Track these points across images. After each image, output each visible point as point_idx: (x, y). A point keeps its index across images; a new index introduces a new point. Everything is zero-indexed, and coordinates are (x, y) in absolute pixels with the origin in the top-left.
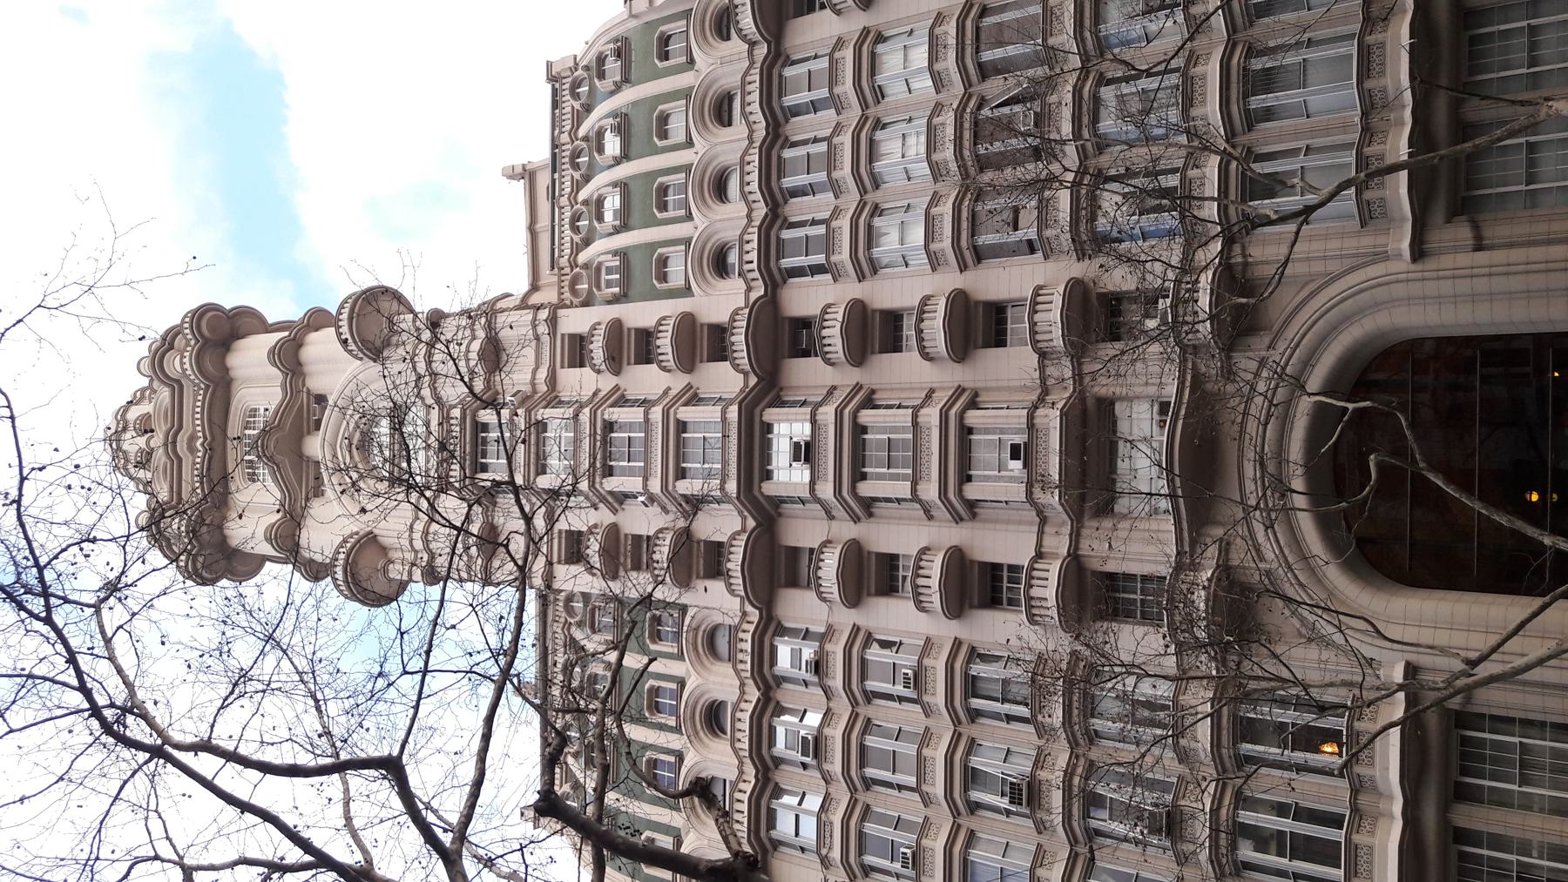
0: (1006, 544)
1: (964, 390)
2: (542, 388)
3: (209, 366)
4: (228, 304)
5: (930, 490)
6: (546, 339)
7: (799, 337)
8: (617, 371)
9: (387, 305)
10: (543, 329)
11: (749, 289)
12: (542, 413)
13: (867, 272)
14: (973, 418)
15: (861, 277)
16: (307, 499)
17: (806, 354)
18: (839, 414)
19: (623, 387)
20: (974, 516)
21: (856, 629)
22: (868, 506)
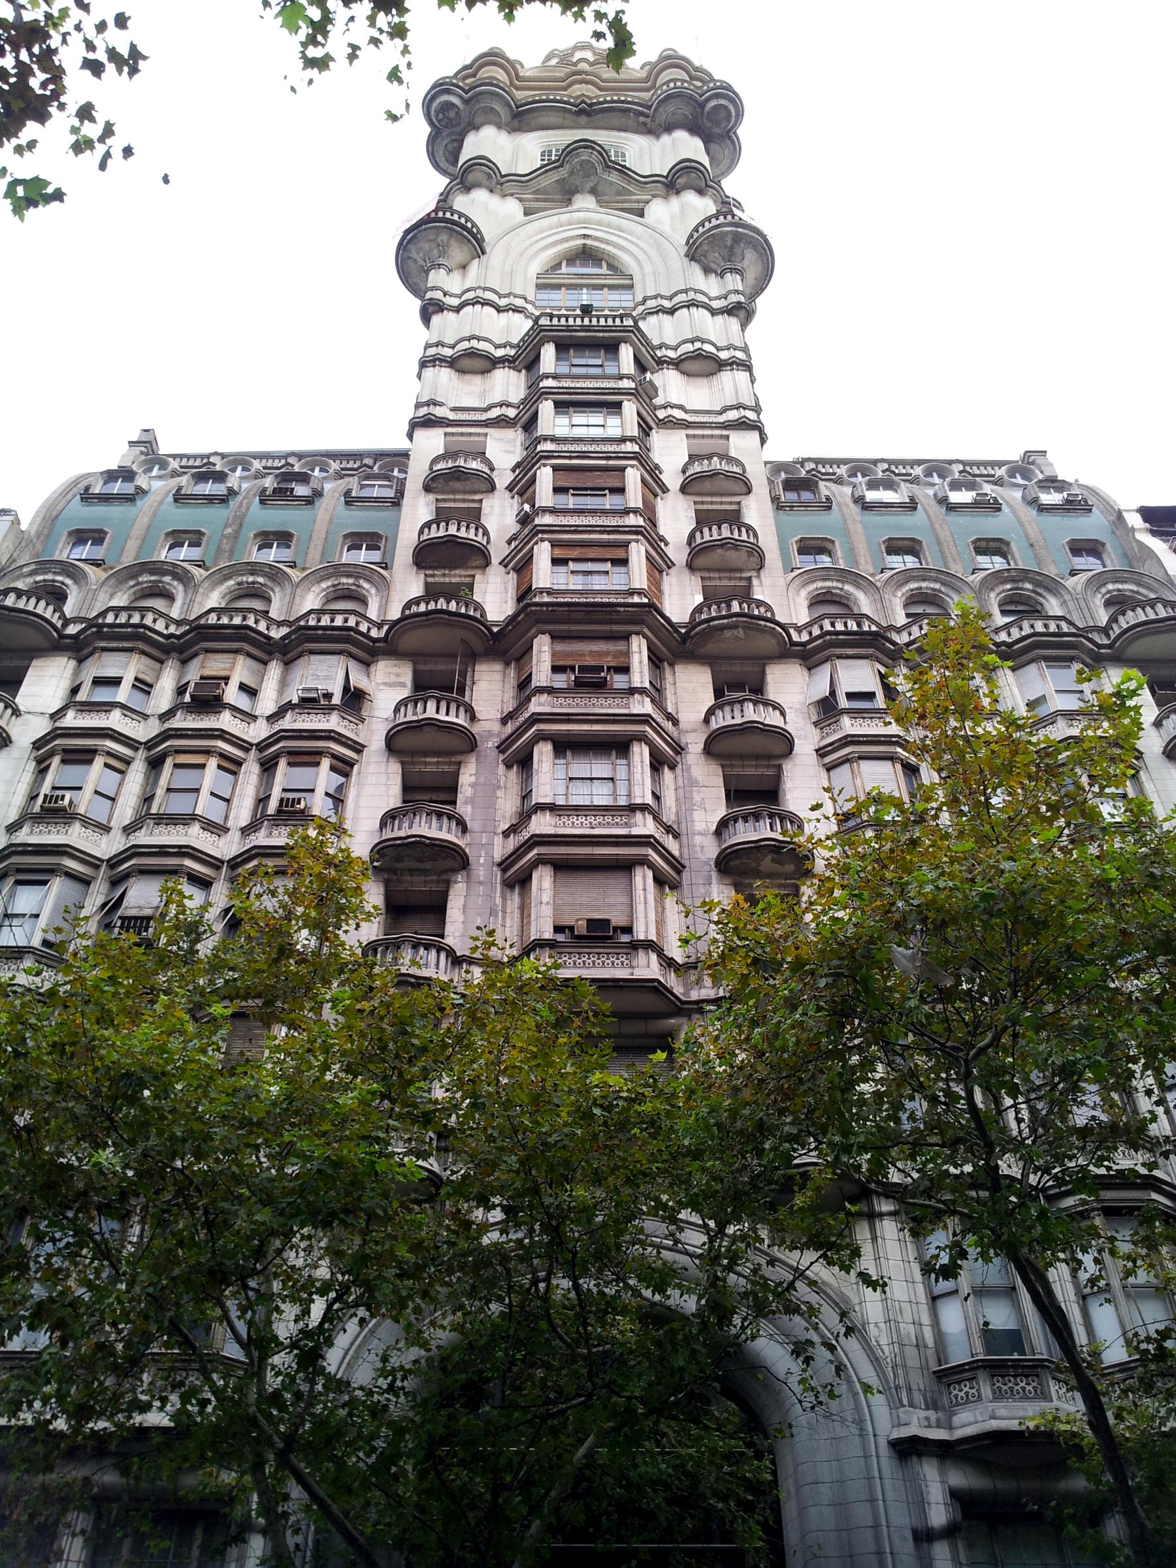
0: (470, 913)
1: (679, 872)
2: (661, 414)
3: (670, 108)
4: (742, 131)
5: (542, 824)
6: (721, 419)
7: (739, 682)
8: (684, 489)
9: (750, 261)
10: (733, 415)
11: (799, 630)
12: (630, 408)
13: (828, 759)
14: (643, 879)
15: (821, 752)
16: (521, 200)
17: (718, 693)
18: (645, 719)
19: (669, 496)
20: (508, 885)
21: (358, 748)
22: (523, 762)
